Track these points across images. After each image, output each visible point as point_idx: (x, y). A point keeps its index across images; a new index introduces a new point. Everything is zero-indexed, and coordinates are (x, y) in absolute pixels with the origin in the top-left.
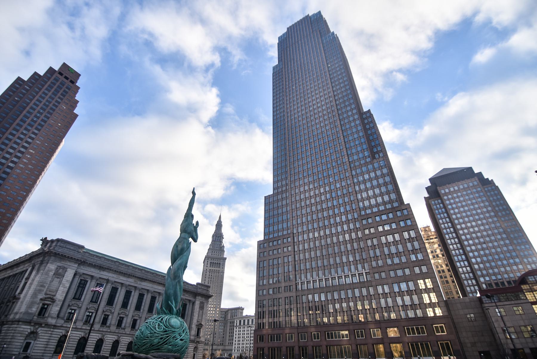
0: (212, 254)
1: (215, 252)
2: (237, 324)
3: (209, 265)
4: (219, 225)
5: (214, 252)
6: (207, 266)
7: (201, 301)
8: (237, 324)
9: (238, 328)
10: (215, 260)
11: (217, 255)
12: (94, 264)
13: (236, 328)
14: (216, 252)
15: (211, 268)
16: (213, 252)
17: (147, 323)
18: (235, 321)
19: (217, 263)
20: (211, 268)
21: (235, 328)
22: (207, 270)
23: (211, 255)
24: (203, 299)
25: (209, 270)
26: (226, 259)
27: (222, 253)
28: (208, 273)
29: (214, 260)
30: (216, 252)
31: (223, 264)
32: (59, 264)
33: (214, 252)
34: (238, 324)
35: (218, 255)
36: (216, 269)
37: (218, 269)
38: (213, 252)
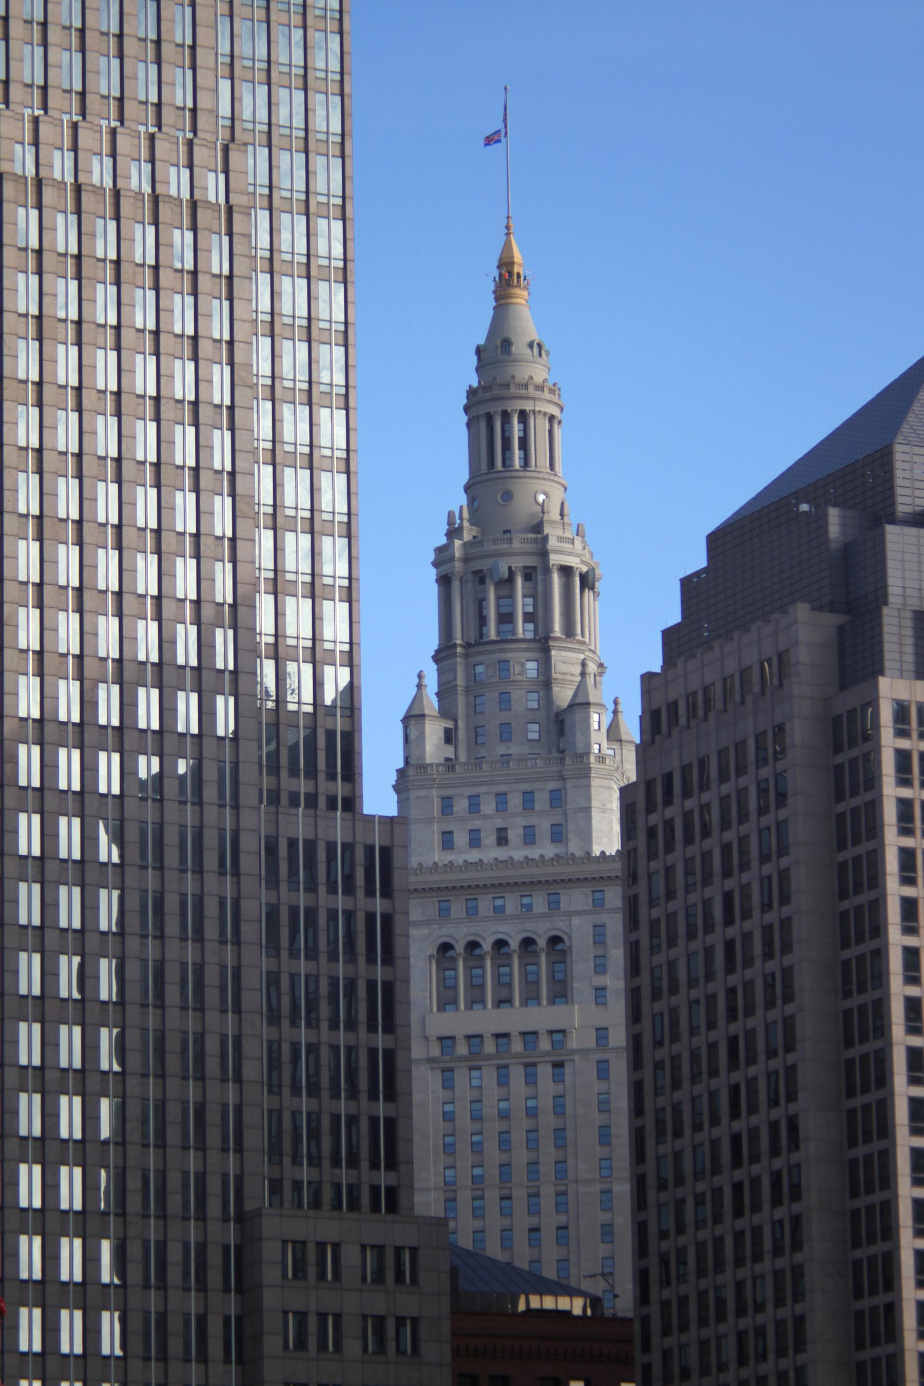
0: (447, 841)
1: (488, 807)
5: (474, 804)
10: (458, 908)
14: (502, 800)
16: (461, 805)
23: (438, 856)
25: (435, 1051)
27: (573, 798)
29: (472, 912)
30: (502, 800)
33: (474, 804)
38: (461, 805)
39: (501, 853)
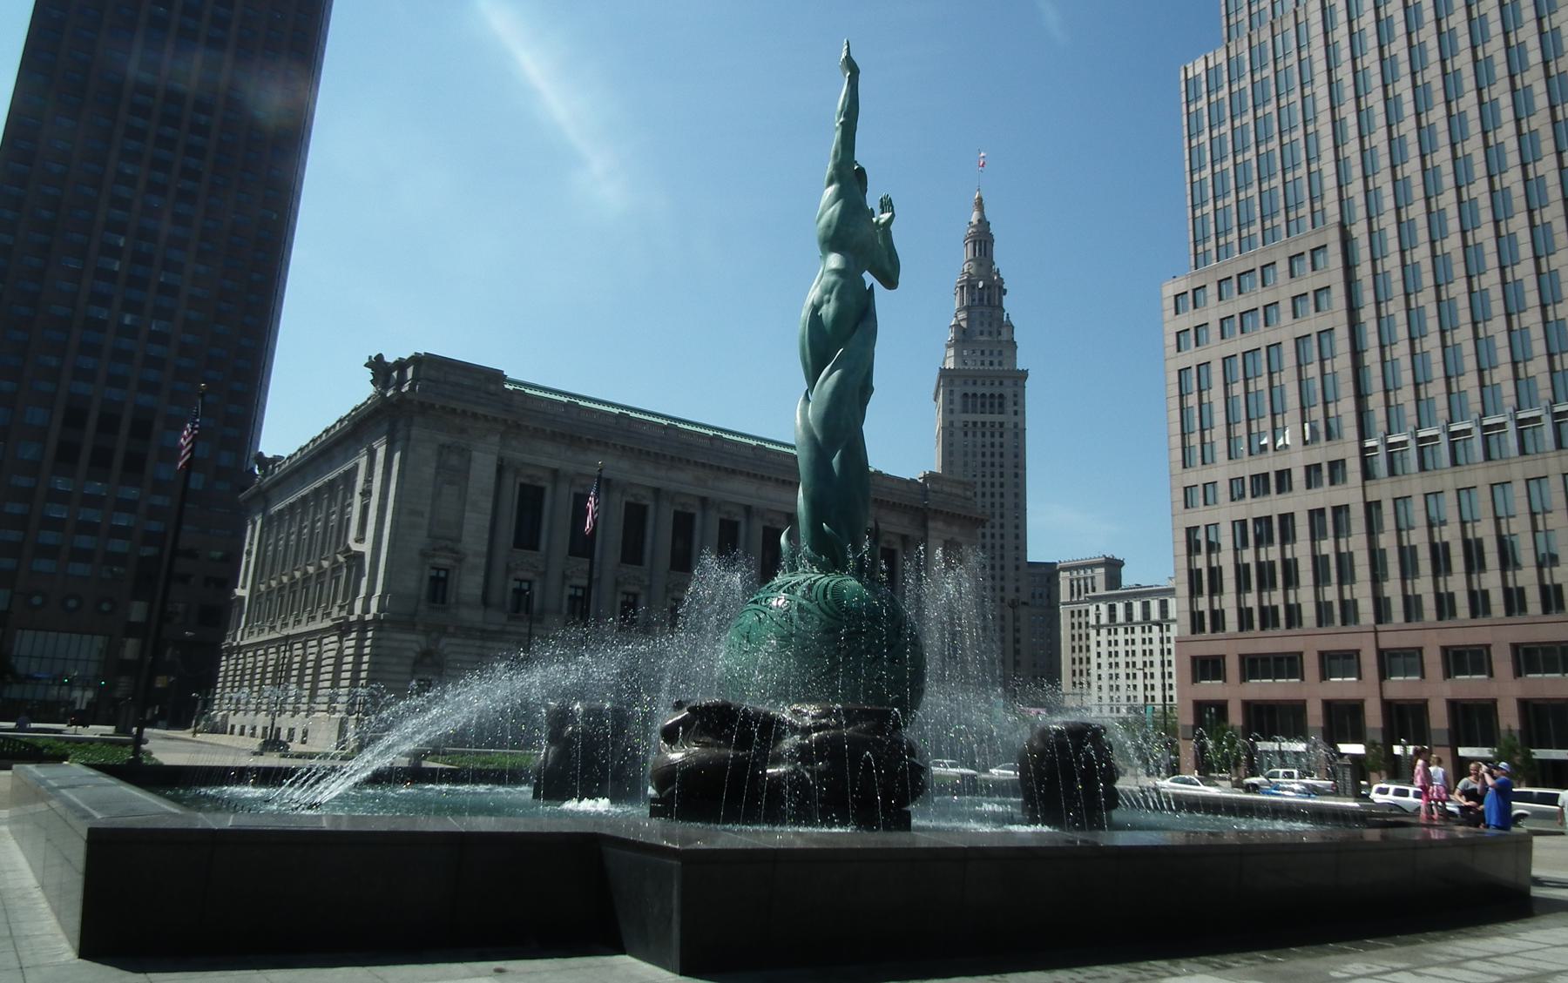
2: (1098, 618)
3: (958, 406)
4: (982, 240)
6: (952, 411)
7: (948, 537)
8: (1098, 618)
9: (1104, 632)
11: (987, 363)
12: (548, 429)
13: (1098, 634)
15: (971, 417)
17: (755, 602)
18: (1092, 609)
19: (992, 396)
20: (971, 417)
21: (1093, 633)
22: (952, 424)
24: (955, 529)
25: (961, 425)
26: (1024, 375)
28: (959, 435)
31: (1015, 396)
32: (443, 438)
34: (1104, 619)
35: (991, 363)
36: (988, 418)
37: (997, 418)
39: (981, 368)
